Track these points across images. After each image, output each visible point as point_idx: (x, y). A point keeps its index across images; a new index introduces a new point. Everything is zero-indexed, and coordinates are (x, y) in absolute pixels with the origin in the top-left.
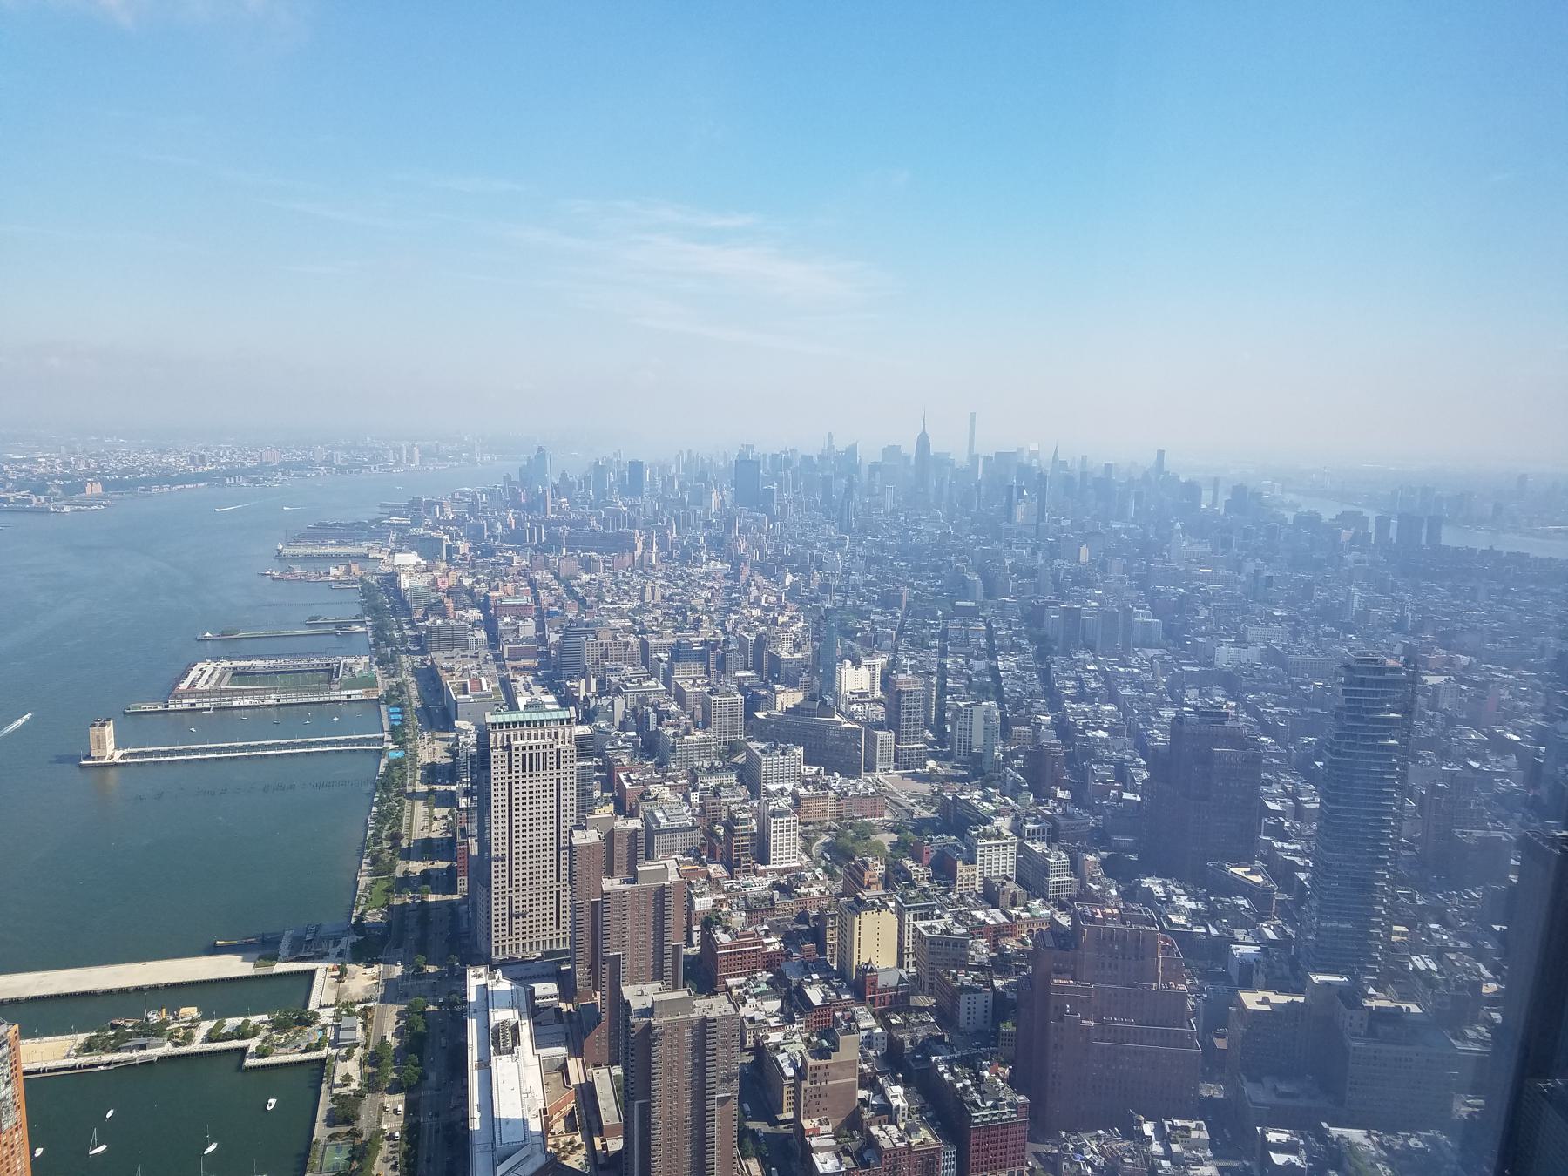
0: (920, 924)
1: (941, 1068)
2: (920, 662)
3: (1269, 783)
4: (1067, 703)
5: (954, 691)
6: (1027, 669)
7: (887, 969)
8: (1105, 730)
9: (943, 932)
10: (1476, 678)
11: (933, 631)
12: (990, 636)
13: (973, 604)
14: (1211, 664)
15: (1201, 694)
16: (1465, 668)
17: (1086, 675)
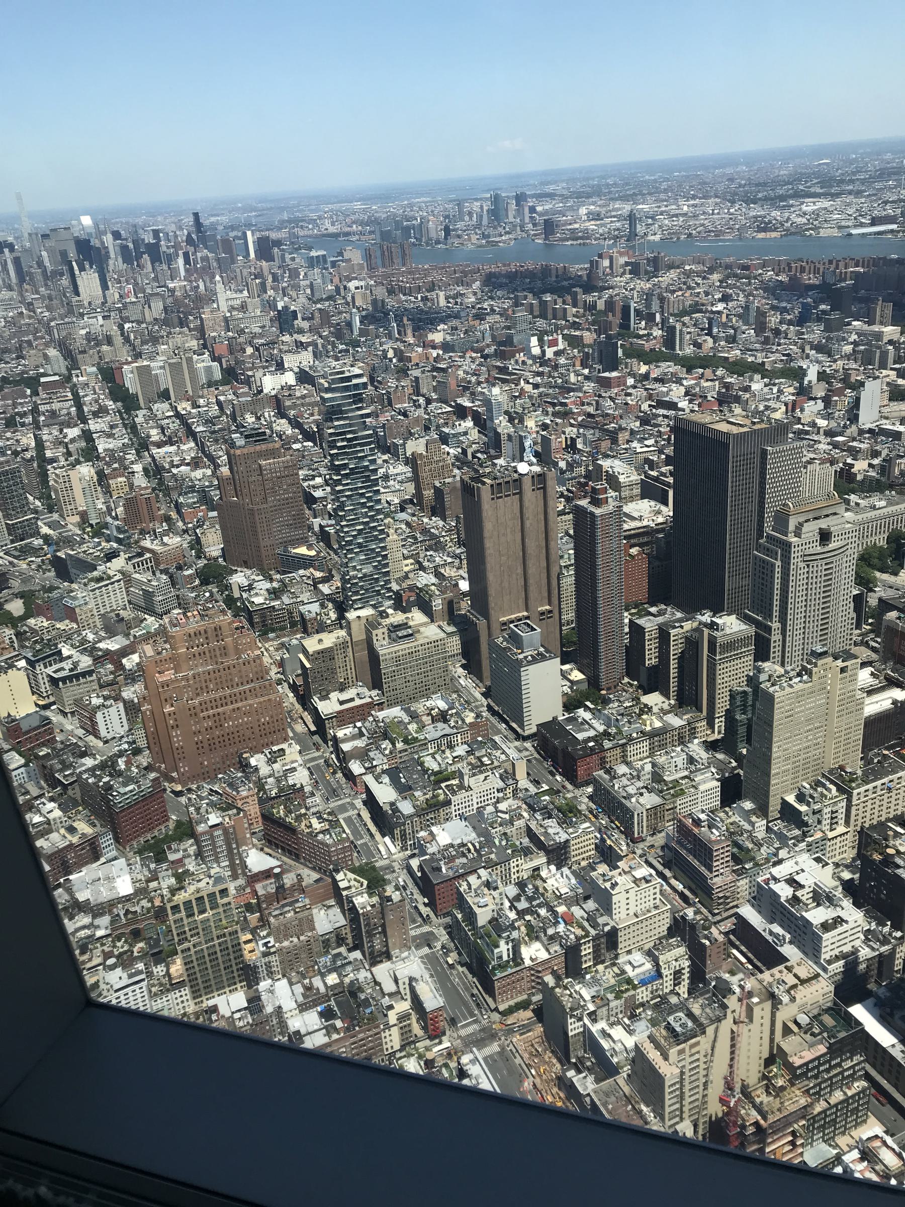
0: (50, 670)
1: (85, 776)
2: (17, 441)
3: (313, 477)
4: (154, 450)
5: (53, 460)
6: (116, 426)
7: (28, 715)
8: (188, 464)
9: (71, 670)
10: (442, 365)
12: (79, 404)
13: (57, 378)
14: (262, 391)
15: (258, 418)
16: (437, 359)
17: (166, 421)
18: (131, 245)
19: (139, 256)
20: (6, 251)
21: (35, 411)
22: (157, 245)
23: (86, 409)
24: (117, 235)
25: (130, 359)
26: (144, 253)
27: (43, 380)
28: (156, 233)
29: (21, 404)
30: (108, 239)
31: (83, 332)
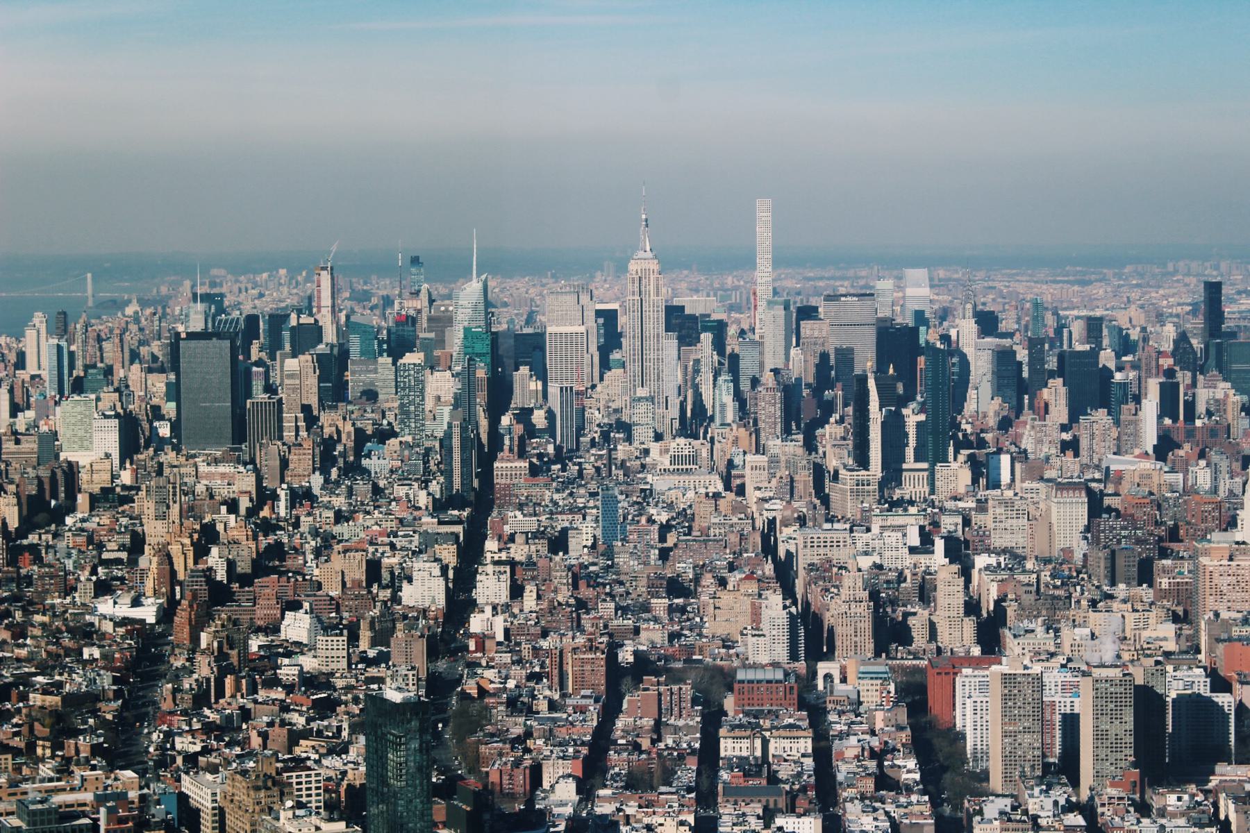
11: (685, 746)
12: (823, 755)
13: (779, 675)
18: (1022, 355)
19: (1041, 378)
20: (706, 338)
21: (709, 755)
22: (1094, 354)
23: (843, 771)
24: (987, 323)
25: (976, 651)
26: (1052, 375)
27: (741, 675)
28: (1094, 327)
29: (676, 730)
30: (965, 331)
31: (866, 562)
